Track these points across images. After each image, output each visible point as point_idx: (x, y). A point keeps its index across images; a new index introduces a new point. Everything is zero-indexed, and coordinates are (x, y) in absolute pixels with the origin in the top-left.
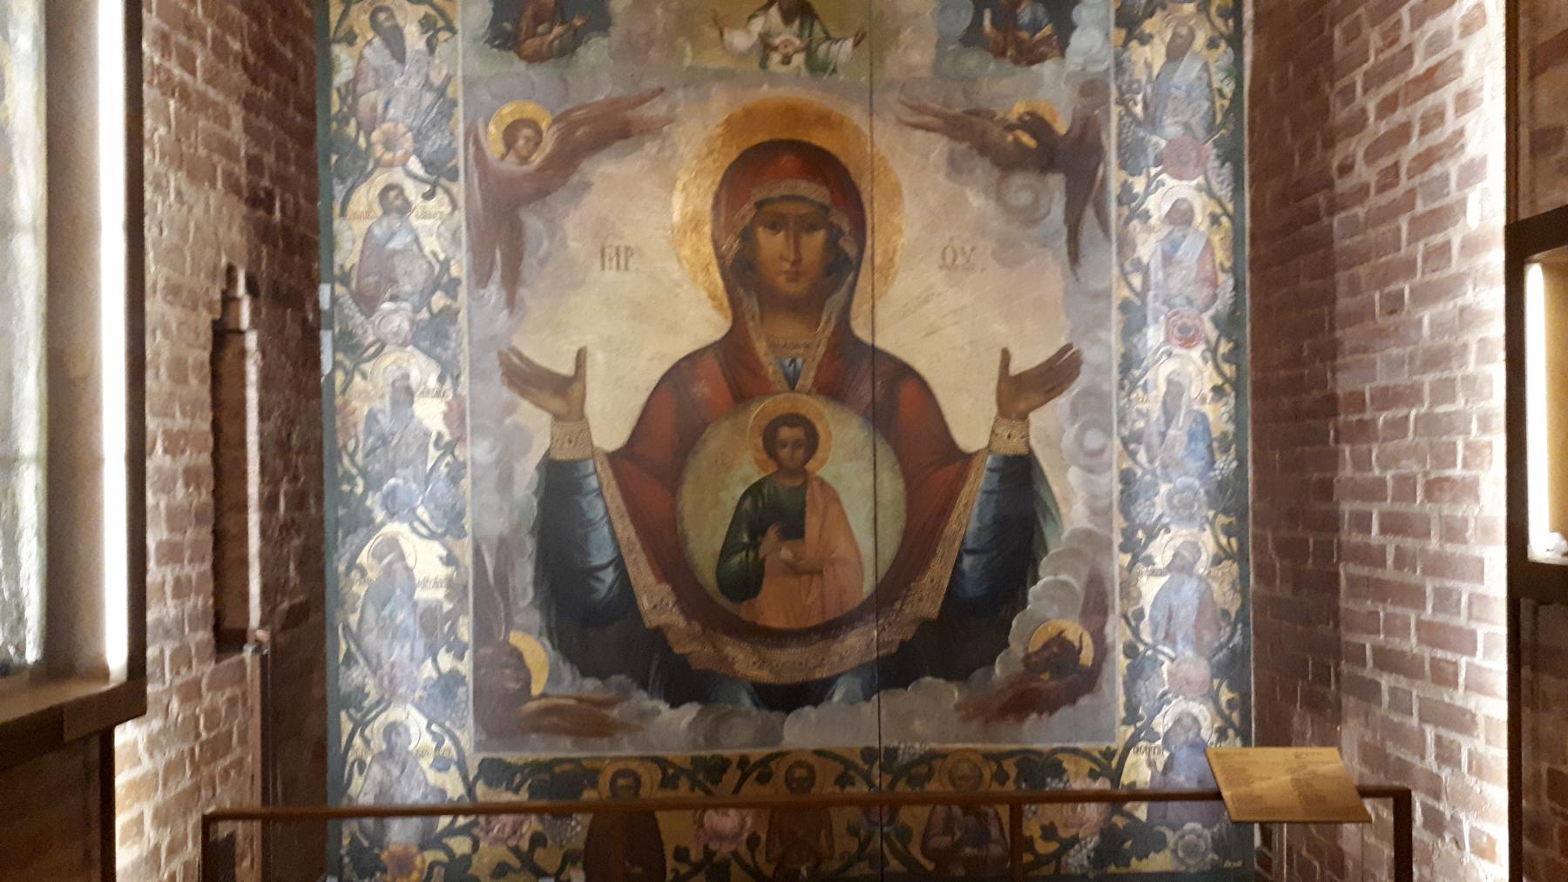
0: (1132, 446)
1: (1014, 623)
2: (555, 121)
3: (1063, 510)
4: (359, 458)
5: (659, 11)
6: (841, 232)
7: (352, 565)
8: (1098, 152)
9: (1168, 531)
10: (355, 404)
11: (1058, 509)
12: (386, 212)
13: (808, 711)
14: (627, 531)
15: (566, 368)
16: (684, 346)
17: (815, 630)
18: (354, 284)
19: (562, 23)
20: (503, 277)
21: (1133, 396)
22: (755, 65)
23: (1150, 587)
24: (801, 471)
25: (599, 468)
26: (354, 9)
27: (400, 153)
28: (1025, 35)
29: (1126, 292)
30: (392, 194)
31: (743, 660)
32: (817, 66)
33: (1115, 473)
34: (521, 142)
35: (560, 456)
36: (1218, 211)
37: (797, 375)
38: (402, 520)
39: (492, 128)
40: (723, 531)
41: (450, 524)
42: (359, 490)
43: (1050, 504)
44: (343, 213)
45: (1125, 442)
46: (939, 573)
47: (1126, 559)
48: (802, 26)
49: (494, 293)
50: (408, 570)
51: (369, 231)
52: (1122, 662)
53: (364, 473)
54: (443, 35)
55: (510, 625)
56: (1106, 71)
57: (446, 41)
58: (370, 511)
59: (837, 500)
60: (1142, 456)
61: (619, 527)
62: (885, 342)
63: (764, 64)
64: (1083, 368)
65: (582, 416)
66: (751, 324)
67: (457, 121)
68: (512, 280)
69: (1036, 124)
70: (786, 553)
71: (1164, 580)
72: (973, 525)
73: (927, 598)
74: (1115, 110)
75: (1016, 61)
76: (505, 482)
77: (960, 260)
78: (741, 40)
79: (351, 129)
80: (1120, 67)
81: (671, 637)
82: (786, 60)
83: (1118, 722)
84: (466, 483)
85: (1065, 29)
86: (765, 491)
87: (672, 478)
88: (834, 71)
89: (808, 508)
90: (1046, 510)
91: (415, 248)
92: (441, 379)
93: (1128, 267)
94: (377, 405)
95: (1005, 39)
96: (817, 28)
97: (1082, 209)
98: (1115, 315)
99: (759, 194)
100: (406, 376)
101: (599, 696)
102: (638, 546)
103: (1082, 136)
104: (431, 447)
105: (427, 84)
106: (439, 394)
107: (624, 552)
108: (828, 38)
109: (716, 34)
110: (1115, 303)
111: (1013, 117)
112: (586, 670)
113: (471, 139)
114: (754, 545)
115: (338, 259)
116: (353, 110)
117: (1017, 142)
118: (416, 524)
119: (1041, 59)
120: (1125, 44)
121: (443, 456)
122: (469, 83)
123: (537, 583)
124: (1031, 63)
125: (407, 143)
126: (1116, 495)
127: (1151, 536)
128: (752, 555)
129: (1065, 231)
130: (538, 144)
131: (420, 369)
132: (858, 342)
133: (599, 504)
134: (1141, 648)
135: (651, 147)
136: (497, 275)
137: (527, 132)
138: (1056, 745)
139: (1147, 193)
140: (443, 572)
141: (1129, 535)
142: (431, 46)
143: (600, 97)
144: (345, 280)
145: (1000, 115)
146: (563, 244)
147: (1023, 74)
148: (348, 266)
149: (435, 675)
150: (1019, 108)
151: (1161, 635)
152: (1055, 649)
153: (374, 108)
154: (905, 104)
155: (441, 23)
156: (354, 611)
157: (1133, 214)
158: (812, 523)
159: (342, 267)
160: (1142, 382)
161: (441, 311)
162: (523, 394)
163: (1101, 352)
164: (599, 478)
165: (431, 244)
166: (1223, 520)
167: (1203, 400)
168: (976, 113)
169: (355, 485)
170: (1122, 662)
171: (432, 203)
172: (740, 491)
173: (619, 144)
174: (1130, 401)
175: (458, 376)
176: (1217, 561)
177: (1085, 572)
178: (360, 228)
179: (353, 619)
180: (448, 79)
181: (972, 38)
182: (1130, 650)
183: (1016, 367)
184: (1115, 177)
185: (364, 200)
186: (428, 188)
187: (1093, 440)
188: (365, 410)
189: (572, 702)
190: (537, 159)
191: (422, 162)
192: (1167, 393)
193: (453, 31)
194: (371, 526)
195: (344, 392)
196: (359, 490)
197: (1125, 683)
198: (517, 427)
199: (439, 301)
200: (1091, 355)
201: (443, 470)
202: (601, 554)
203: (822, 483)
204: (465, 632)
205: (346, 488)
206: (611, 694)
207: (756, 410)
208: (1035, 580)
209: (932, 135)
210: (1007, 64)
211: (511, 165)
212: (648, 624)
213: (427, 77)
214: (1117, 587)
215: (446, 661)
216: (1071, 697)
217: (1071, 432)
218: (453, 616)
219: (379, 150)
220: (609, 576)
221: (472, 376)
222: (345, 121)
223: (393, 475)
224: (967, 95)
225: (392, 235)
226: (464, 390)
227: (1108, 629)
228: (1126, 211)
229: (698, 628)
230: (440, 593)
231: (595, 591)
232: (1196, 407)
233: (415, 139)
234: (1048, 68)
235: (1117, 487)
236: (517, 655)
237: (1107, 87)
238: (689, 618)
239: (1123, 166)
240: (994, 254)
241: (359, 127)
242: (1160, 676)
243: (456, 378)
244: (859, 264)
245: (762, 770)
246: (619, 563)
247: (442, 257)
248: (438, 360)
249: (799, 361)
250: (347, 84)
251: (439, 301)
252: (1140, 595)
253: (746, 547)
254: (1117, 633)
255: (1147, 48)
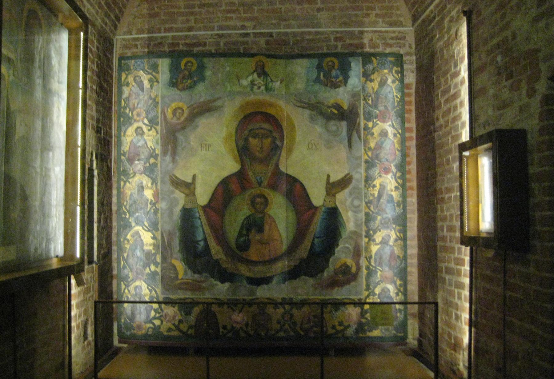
0: (369, 205)
1: (331, 260)
2: (188, 107)
3: (347, 224)
4: (128, 207)
5: (220, 75)
6: (275, 138)
7: (125, 239)
8: (357, 115)
9: (380, 231)
10: (127, 191)
11: (345, 225)
12: (137, 135)
13: (265, 286)
14: (207, 229)
15: (189, 180)
16: (226, 174)
17: (268, 261)
18: (127, 156)
19: (191, 79)
20: (171, 154)
21: (369, 189)
22: (249, 89)
23: (374, 249)
24: (262, 212)
25: (199, 210)
26: (129, 76)
27: (142, 118)
28: (333, 80)
29: (366, 157)
30: (139, 130)
31: (244, 270)
32: (268, 89)
33: (363, 213)
34: (178, 114)
35: (187, 207)
36: (396, 132)
37: (261, 182)
38: (140, 225)
39: (169, 110)
40: (238, 230)
41: (154, 227)
42: (127, 217)
43: (342, 222)
44: (124, 135)
45: (366, 203)
46: (307, 244)
47: (367, 240)
48: (264, 78)
49: (168, 158)
50: (142, 240)
51: (132, 141)
52: (365, 272)
53: (129, 212)
54: (155, 84)
55: (172, 257)
56: (359, 91)
57: (156, 85)
58: (130, 223)
59: (275, 222)
60: (372, 208)
61: (205, 228)
62: (291, 172)
63: (252, 89)
64: (353, 181)
65: (194, 195)
66: (247, 167)
67: (159, 109)
68: (174, 154)
69: (338, 106)
70: (258, 237)
71: (378, 246)
72: (318, 229)
73: (303, 252)
74: (362, 102)
75: (331, 88)
76: (171, 213)
77: (314, 147)
78: (245, 82)
79: (127, 111)
80: (364, 89)
81: (221, 262)
82: (259, 88)
83: (363, 290)
84: (159, 215)
85: (346, 78)
86: (251, 218)
87: (221, 213)
88: (274, 91)
89: (265, 224)
90: (341, 224)
91: (145, 145)
92: (152, 184)
93: (367, 150)
94: (133, 191)
95: (327, 80)
96: (269, 78)
97: (352, 133)
98: (363, 164)
99: (251, 127)
100: (142, 183)
101: (199, 279)
102: (211, 235)
103: (352, 109)
104: (149, 204)
105: (150, 98)
106: (151, 188)
107: (207, 236)
108: (272, 81)
109: (238, 81)
110: (363, 160)
111: (330, 104)
112: (195, 271)
113: (163, 113)
114: (248, 235)
115: (122, 149)
116: (128, 105)
117: (332, 112)
118: (144, 227)
119: (339, 86)
120: (365, 83)
121: (152, 207)
122: (163, 97)
123: (180, 244)
124: (335, 88)
125: (144, 114)
126: (363, 220)
127: (375, 232)
128: (247, 238)
129: (347, 138)
130: (182, 115)
131: (146, 181)
132: (282, 172)
133: (199, 221)
134: (371, 267)
135: (216, 114)
136: (169, 153)
137: (180, 111)
138: (343, 297)
139: (373, 128)
140: (152, 241)
141: (367, 232)
142: (152, 87)
143: (202, 100)
144: (124, 154)
145: (326, 103)
146: (189, 143)
147: (333, 92)
148: (125, 150)
149: (149, 272)
150: (332, 101)
151: (377, 263)
152: (344, 268)
153: (134, 105)
154: (296, 100)
155: (155, 80)
156: (125, 252)
157: (368, 134)
158: (266, 228)
159: (123, 151)
160: (372, 185)
161: (152, 164)
162: (177, 188)
163: (359, 175)
164: (199, 214)
165: (150, 144)
166: (398, 228)
167: (392, 190)
168: (319, 103)
169: (126, 215)
170: (365, 272)
171: (151, 132)
172: (243, 218)
173: (207, 114)
174: (368, 191)
175: (158, 182)
176: (396, 240)
177: (353, 243)
178: (129, 139)
179: (125, 255)
180: (157, 96)
181: (317, 80)
182: (368, 268)
183: (332, 180)
184: (362, 122)
185: (130, 131)
186: (150, 128)
187: (356, 203)
188: (130, 193)
189: (190, 281)
190: (182, 119)
191: (148, 120)
192: (380, 188)
193: (158, 82)
194: (130, 227)
195: (123, 188)
196: (127, 217)
197: (366, 279)
198: (174, 197)
199: (152, 161)
200: (356, 176)
201: (152, 211)
202: (200, 237)
203: (269, 216)
204: (159, 259)
205: (123, 216)
206: (202, 279)
207: (248, 193)
208: (338, 246)
209: (304, 110)
210: (328, 89)
211: (175, 121)
212: (214, 259)
213: (150, 95)
214: (364, 248)
215: (153, 268)
216: (348, 282)
217: (349, 200)
218: (155, 255)
219: (135, 117)
220: (202, 243)
221: (161, 182)
222: (125, 108)
223: (138, 212)
224: (315, 97)
225: (139, 141)
226: (159, 187)
227: (361, 261)
228: (366, 132)
229: (230, 260)
230: (151, 248)
231: (197, 247)
232: (389, 193)
233: (146, 113)
234: (341, 90)
235: (364, 218)
236: (174, 266)
237: (360, 95)
238: (226, 256)
239: (365, 119)
240: (325, 145)
241: (130, 110)
242: (377, 276)
243: (156, 184)
244: (282, 148)
245: (250, 304)
246: (205, 240)
247: (153, 148)
248: (152, 178)
249: (262, 178)
250: (126, 98)
251: (152, 161)
252: (371, 251)
253: (245, 235)
254: (363, 262)
255: (373, 83)
